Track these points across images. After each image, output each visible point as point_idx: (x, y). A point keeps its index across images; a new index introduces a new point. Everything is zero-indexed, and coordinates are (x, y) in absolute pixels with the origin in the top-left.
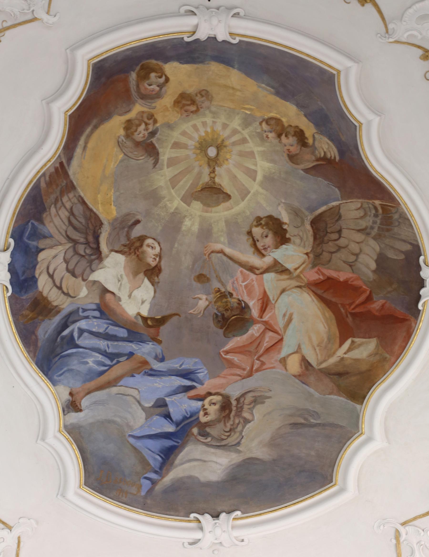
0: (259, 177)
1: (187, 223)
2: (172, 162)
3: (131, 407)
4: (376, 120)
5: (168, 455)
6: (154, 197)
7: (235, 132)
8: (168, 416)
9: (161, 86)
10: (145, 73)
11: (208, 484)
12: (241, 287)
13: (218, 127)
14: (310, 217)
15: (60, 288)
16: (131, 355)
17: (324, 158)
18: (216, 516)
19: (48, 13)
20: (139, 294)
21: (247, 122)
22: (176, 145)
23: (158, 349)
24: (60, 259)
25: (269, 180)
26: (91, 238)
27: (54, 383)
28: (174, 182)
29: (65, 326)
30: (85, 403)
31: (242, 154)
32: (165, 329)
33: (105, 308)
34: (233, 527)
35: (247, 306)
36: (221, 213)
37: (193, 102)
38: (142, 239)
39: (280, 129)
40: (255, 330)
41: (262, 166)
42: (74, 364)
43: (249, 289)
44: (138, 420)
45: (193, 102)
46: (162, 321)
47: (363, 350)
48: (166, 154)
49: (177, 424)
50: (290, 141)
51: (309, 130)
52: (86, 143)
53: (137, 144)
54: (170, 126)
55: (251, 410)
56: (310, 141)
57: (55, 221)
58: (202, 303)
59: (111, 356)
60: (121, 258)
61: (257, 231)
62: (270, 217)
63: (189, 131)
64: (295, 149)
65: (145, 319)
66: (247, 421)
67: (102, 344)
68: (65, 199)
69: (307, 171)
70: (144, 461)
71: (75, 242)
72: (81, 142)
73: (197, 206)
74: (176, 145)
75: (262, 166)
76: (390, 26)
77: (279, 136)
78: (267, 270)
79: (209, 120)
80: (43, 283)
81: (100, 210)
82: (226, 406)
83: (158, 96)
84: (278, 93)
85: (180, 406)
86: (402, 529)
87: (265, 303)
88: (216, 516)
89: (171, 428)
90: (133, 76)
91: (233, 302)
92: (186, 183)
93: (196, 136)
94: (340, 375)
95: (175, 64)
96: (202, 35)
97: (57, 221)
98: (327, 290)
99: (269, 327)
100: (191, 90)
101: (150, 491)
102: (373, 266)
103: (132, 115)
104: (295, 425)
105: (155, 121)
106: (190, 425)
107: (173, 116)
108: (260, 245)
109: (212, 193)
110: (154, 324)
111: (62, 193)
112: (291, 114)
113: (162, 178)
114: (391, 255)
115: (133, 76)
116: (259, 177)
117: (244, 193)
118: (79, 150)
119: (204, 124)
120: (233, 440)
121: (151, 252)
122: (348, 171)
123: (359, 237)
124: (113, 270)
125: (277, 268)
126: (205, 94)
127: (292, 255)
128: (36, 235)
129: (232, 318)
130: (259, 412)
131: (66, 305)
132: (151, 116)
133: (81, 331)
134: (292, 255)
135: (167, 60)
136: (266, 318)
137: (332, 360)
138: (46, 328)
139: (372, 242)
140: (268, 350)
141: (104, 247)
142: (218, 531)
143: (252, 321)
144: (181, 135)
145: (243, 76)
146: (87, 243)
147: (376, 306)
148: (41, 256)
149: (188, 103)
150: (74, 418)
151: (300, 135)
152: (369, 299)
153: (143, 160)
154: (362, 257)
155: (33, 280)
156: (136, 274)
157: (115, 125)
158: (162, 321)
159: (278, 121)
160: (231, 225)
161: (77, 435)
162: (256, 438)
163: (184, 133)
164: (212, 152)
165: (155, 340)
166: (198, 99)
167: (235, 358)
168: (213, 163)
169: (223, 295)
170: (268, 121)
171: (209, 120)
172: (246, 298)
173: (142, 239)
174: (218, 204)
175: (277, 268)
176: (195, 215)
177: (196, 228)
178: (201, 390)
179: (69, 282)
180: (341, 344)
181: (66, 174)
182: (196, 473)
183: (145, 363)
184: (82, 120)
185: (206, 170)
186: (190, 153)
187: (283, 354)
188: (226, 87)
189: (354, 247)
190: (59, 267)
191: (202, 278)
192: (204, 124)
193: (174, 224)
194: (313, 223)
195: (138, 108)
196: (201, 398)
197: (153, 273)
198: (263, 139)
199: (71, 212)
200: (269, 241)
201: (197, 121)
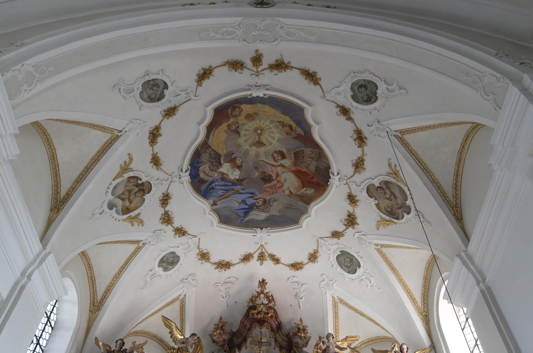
0: (276, 139)
1: (251, 152)
2: (245, 135)
3: (234, 202)
4: (317, 127)
5: (246, 213)
6: (239, 146)
7: (267, 125)
8: (246, 204)
9: (240, 112)
10: (234, 109)
11: (259, 220)
12: (269, 170)
13: (261, 124)
14: (294, 152)
15: (208, 175)
16: (233, 189)
17: (299, 135)
18: (262, 229)
19: (195, 96)
20: (235, 173)
21: (272, 122)
22: (246, 130)
23: (242, 187)
24: (207, 167)
25: (279, 140)
26: (217, 160)
27: (208, 200)
28: (246, 141)
29: (211, 185)
30: (218, 203)
31: (269, 132)
32: (244, 182)
33: (224, 178)
34: (267, 232)
35: (272, 176)
36: (262, 150)
37: (252, 117)
38: (235, 158)
39: (283, 125)
40: (274, 182)
41: (277, 136)
42: (214, 194)
43: (272, 171)
44: (236, 205)
45: (252, 117)
46: (243, 180)
47: (310, 191)
48: (242, 133)
49: (249, 206)
50: (287, 129)
51: (294, 126)
52: (214, 133)
53: (232, 131)
54: (244, 125)
55: (273, 203)
56: (294, 129)
57: (205, 157)
58: (257, 174)
59: (226, 190)
60: (228, 164)
61: (275, 155)
62: (280, 151)
63: (251, 125)
64: (289, 131)
65: (237, 180)
66: (271, 206)
67: (223, 188)
68: (207, 151)
69: (292, 138)
70: (239, 216)
71: (212, 162)
72: (212, 133)
73: (254, 148)
74: (246, 130)
75: (277, 136)
76: (325, 94)
77: (283, 127)
78: (278, 166)
79: (258, 122)
80: (202, 175)
81: (220, 152)
82: (265, 201)
83: (239, 115)
84: (283, 113)
85: (250, 201)
86: (320, 240)
87: (278, 175)
88: (262, 229)
89: (247, 207)
90: (230, 110)
91: (267, 174)
92: (250, 141)
93: (253, 127)
94: (302, 197)
95: (245, 105)
96: (255, 95)
97: (205, 157)
98: (298, 173)
99: (279, 182)
100: (251, 113)
101: (241, 222)
102: (314, 169)
103: (230, 122)
104: (287, 208)
105: (238, 123)
106: (254, 206)
107: (245, 121)
108: (276, 159)
109: (260, 144)
110: (240, 181)
111: (206, 149)
112: (287, 120)
113: (242, 140)
114: (320, 167)
115: (230, 110)
116: (276, 139)
117: (271, 144)
118: (211, 136)
119: (256, 123)
120: (267, 210)
121: (238, 162)
122: (307, 138)
123: (310, 160)
124: (226, 168)
125: (282, 165)
126: (256, 114)
127: (287, 162)
128: (198, 163)
129: (266, 179)
130: (275, 204)
131: (210, 179)
132: (237, 122)
133: (216, 185)
134: (287, 162)
135: (241, 104)
136: (278, 179)
137: (299, 193)
138: (204, 187)
139: (314, 162)
140: (278, 188)
141: (222, 162)
142: (262, 234)
143: (274, 180)
144: (248, 128)
145: (270, 108)
146: (216, 162)
147: (315, 180)
148: (200, 168)
149: (250, 117)
150: (215, 207)
151: (291, 127)
152: (312, 178)
153: (235, 136)
154: (311, 166)
155: (199, 175)
156: (234, 168)
157: (224, 126)
158: (243, 180)
159: (283, 122)
160: (266, 153)
161: (217, 212)
162: (275, 210)
163: (249, 126)
164: (259, 132)
165: (241, 185)
166: (254, 115)
167: (268, 189)
168: (260, 135)
169: (264, 173)
170: (279, 122)
171: (258, 122)
172: (271, 174)
173: (235, 158)
174: (261, 147)
175: (282, 165)
176: (253, 151)
177: (254, 154)
178: (256, 197)
179: (211, 173)
180: (303, 189)
181: (208, 144)
182: (255, 218)
183: (238, 191)
184: (211, 128)
185: (257, 137)
186: (251, 129)
187: (283, 189)
188: (264, 111)
189: (308, 162)
190: (207, 170)
191: (256, 168)
192: (256, 123)
193: (247, 153)
194: (294, 154)
195: (232, 120)
196: (257, 199)
197: (239, 167)
198: (277, 127)
199: (210, 154)
200: (279, 158)
201: (254, 122)
